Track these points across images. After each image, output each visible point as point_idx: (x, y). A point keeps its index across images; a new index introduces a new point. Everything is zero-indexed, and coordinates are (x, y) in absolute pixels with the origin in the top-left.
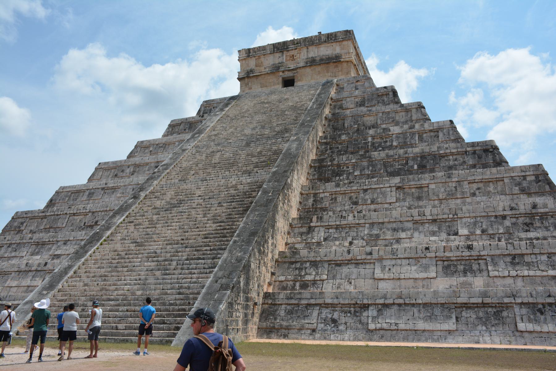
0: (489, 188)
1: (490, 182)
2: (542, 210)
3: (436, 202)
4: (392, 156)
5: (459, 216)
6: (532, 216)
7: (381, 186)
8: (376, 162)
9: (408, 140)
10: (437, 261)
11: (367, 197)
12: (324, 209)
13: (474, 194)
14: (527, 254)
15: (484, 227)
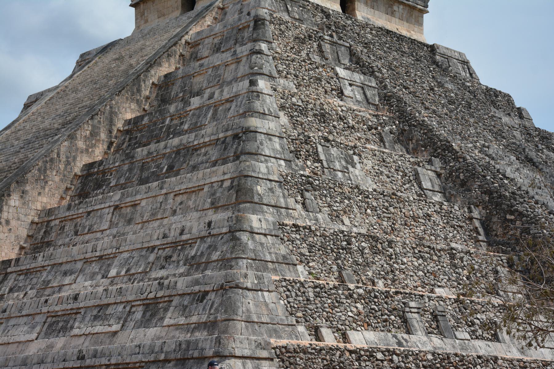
0: (189, 201)
1: (193, 192)
2: (184, 237)
3: (140, 226)
4: (152, 153)
5: (122, 249)
6: (174, 245)
7: (102, 206)
8: (137, 163)
9: (200, 119)
10: (48, 317)
11: (87, 223)
12: (49, 244)
13: (174, 212)
14: (112, 304)
15: (131, 264)
